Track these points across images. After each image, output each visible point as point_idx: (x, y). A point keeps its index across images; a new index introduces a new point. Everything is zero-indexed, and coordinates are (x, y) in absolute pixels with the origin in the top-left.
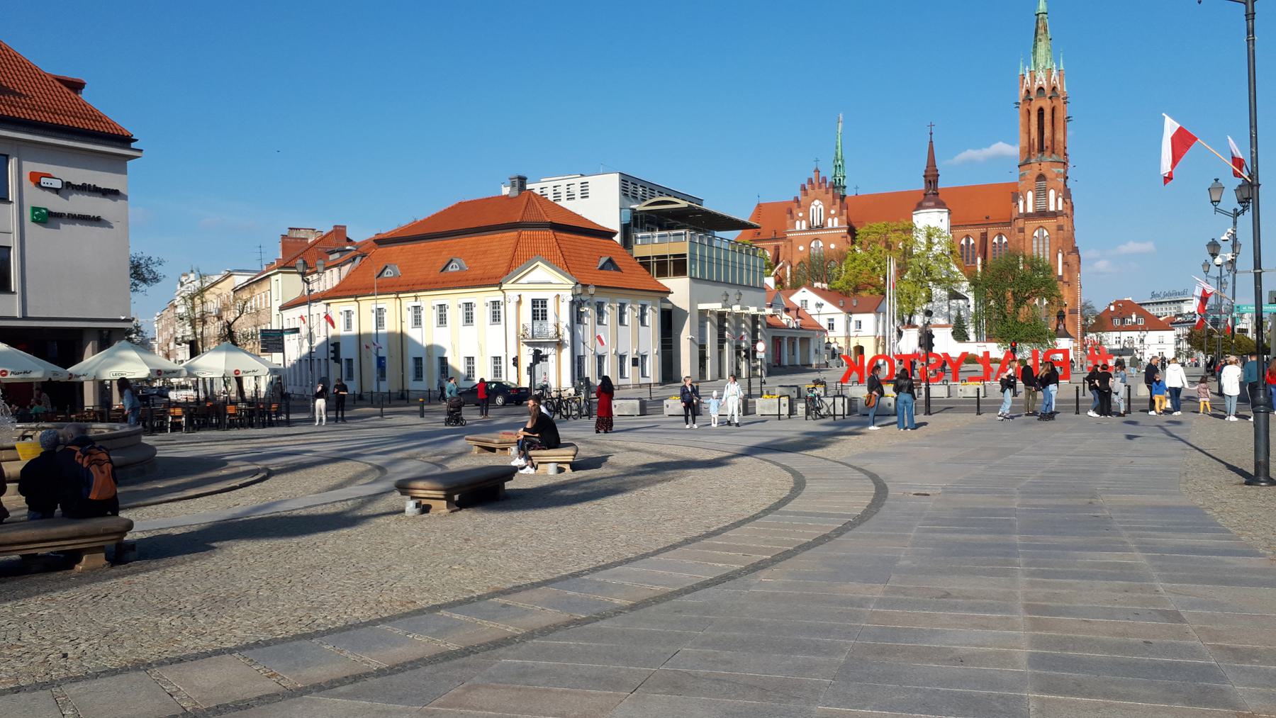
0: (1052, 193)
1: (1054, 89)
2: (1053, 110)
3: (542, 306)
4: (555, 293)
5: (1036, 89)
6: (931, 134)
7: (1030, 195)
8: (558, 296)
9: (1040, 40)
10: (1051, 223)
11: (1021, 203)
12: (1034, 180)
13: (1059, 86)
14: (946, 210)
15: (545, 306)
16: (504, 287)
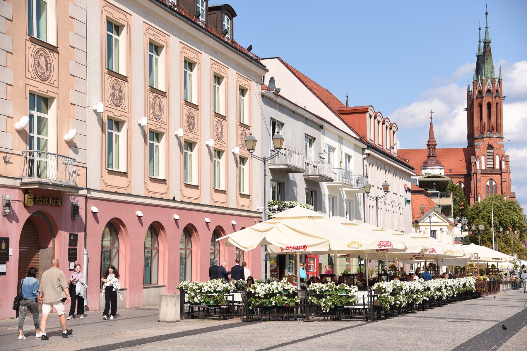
0: (497, 158)
1: (497, 91)
2: (497, 104)
3: (434, 234)
4: (440, 227)
5: (486, 91)
6: (431, 118)
7: (483, 157)
8: (441, 229)
9: (487, 59)
10: (497, 178)
11: (478, 163)
12: (486, 148)
13: (499, 90)
14: (443, 167)
15: (435, 234)
16: (420, 224)
